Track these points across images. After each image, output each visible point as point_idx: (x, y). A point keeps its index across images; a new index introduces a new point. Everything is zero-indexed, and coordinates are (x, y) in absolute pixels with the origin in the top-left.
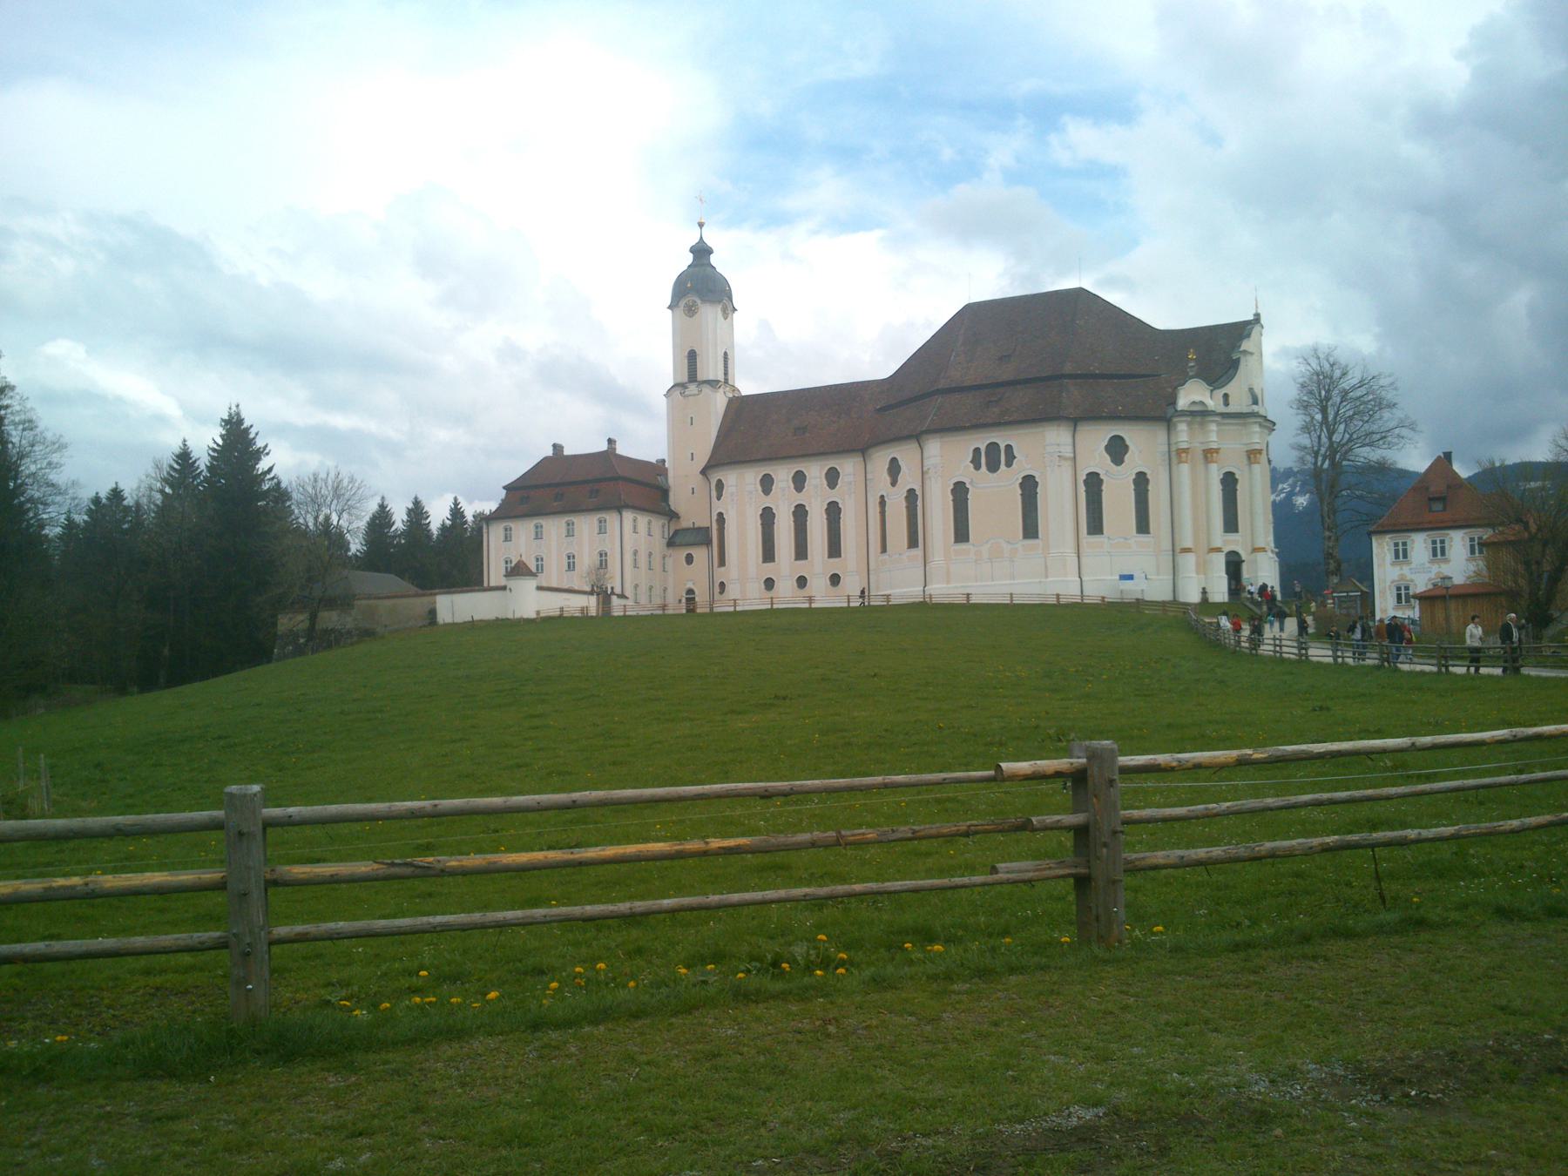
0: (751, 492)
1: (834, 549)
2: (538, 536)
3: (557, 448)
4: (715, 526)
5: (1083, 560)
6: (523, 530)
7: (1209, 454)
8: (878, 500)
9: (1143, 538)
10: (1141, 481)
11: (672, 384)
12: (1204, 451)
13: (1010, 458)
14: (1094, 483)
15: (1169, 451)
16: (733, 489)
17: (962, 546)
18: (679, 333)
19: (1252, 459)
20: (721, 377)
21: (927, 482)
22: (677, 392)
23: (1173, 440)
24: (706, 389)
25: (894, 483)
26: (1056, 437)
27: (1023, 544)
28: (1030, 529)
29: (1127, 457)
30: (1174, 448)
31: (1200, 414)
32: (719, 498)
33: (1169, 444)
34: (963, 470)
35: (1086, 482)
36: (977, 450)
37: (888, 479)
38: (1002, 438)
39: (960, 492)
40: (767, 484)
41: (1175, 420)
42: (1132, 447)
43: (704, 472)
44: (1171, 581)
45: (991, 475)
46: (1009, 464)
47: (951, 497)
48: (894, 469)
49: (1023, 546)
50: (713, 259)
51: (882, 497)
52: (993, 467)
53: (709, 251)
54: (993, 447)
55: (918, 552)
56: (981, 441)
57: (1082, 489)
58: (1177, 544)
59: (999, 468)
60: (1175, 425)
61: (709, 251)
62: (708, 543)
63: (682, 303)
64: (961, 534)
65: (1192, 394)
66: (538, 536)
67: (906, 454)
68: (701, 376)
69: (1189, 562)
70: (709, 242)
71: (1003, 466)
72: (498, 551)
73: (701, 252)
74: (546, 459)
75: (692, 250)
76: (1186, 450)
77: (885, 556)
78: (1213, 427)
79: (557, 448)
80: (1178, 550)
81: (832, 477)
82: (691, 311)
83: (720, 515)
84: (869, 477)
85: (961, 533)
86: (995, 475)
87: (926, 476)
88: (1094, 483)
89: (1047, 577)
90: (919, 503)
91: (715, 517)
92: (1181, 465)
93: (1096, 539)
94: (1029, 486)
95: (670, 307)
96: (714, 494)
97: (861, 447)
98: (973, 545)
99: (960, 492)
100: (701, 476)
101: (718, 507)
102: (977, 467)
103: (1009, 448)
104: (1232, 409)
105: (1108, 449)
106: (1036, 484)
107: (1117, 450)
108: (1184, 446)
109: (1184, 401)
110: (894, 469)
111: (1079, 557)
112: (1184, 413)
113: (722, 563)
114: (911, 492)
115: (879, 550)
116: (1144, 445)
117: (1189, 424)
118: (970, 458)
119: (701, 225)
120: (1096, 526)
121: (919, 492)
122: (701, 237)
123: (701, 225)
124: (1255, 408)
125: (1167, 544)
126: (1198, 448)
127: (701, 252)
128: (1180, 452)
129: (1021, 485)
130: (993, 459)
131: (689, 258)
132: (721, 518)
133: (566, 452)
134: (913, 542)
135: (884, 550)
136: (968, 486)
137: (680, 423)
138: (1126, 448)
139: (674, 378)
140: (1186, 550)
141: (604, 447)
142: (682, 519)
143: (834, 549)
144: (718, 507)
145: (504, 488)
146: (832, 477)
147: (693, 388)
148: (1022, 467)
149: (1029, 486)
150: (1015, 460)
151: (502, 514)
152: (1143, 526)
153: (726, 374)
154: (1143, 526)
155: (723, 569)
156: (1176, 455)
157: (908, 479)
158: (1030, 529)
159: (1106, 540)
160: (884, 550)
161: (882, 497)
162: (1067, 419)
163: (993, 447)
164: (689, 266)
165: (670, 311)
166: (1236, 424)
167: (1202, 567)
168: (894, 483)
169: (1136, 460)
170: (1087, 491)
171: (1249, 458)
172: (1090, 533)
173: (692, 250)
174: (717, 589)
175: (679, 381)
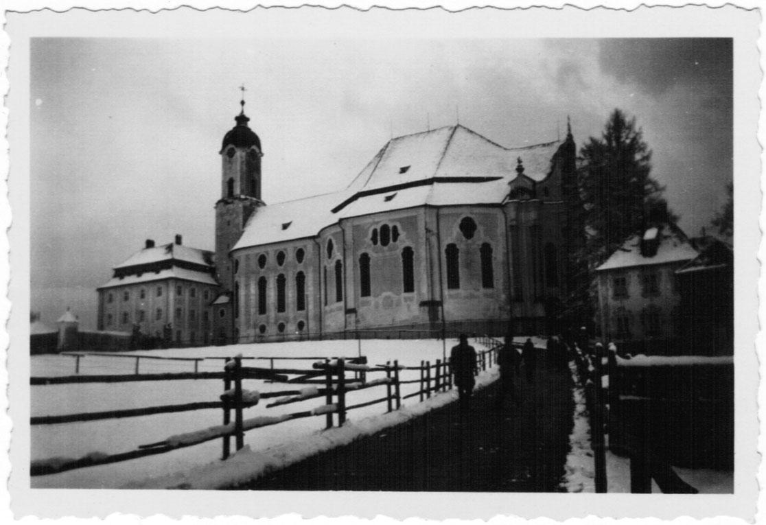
1: (301, 304)
22: (222, 204)
35: (447, 251)
46: (395, 239)
50: (250, 125)
52: (385, 242)
53: (248, 119)
57: (444, 256)
59: (388, 242)
61: (248, 119)
63: (226, 150)
70: (247, 114)
71: (391, 242)
73: (242, 120)
75: (237, 119)
88: (452, 250)
90: (342, 270)
94: (408, 254)
102: (375, 242)
105: (462, 227)
106: (412, 253)
114: (338, 263)
119: (243, 103)
121: (342, 262)
122: (242, 112)
123: (243, 103)
127: (242, 120)
131: (234, 124)
143: (301, 304)
148: (404, 241)
149: (408, 254)
157: (337, 255)
169: (480, 236)
170: (447, 258)
172: (449, 287)
173: (237, 119)
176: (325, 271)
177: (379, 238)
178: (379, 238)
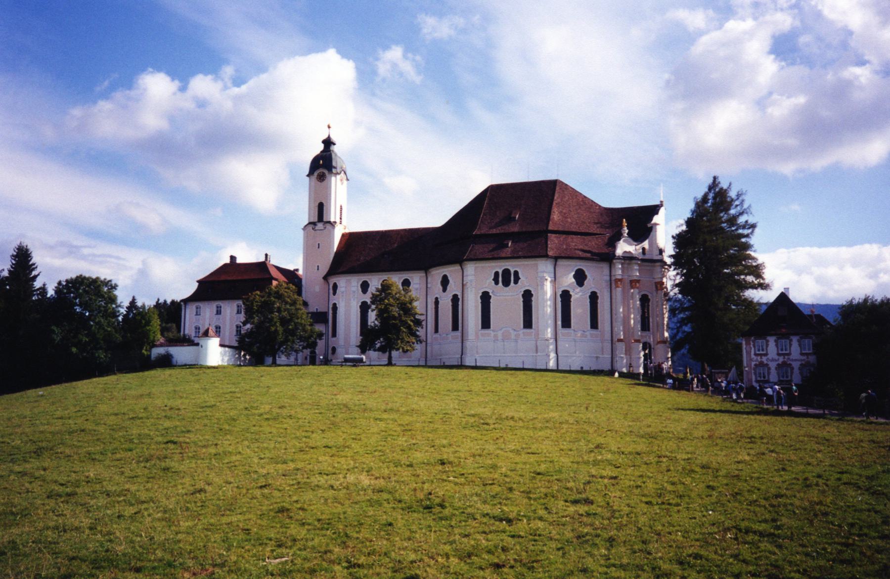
0: (354, 292)
2: (219, 312)
3: (233, 258)
4: (331, 312)
5: (559, 343)
6: (208, 310)
7: (633, 283)
8: (434, 300)
9: (594, 332)
10: (594, 297)
11: (306, 222)
12: (631, 281)
13: (516, 281)
14: (566, 297)
15: (611, 280)
16: (343, 289)
17: (486, 331)
18: (313, 193)
19: (659, 288)
20: (338, 221)
21: (465, 290)
22: (311, 227)
23: (613, 273)
24: (328, 226)
25: (444, 290)
26: (544, 267)
27: (523, 332)
28: (528, 323)
29: (586, 282)
30: (613, 278)
31: (628, 258)
32: (334, 293)
33: (611, 276)
34: (488, 285)
35: (561, 296)
36: (497, 274)
37: (441, 288)
38: (512, 266)
39: (486, 298)
40: (365, 287)
41: (614, 261)
42: (589, 277)
43: (326, 278)
44: (610, 359)
45: (505, 289)
46: (516, 282)
47: (480, 301)
48: (445, 282)
49: (523, 333)
50: (335, 149)
51: (437, 299)
52: (506, 283)
54: (506, 272)
55: (458, 334)
56: (499, 266)
57: (559, 299)
58: (614, 336)
60: (614, 264)
62: (325, 321)
63: (316, 174)
64: (486, 323)
65: (624, 247)
66: (219, 312)
67: (452, 271)
68: (325, 220)
69: (621, 348)
70: (334, 138)
72: (190, 321)
73: (328, 143)
74: (225, 265)
75: (324, 142)
76: (620, 280)
77: (437, 335)
78: (636, 267)
79: (233, 258)
80: (615, 339)
81: (406, 283)
82: (322, 178)
83: (335, 305)
84: (429, 286)
85: (486, 323)
86: (507, 289)
87: (465, 287)
88: (566, 297)
89: (537, 353)
90: (460, 303)
91: (331, 306)
92: (618, 289)
93: (566, 331)
94: (527, 296)
95: (308, 176)
96: (331, 291)
97: (425, 265)
98: (493, 331)
99: (486, 298)
100: (322, 280)
101: (334, 299)
102: (497, 283)
103: (516, 273)
104: (647, 257)
106: (532, 295)
107: (580, 278)
108: (619, 277)
109: (619, 251)
110: (445, 282)
111: (556, 341)
112: (619, 258)
113: (334, 334)
115: (433, 330)
116: (596, 275)
117: (622, 264)
118: (493, 277)
119: (329, 127)
120: (566, 322)
121: (460, 297)
124: (659, 257)
125: (608, 336)
126: (627, 280)
127: (328, 143)
128: (617, 280)
129: (523, 296)
130: (506, 278)
131: (321, 147)
132: (335, 308)
133: (239, 261)
134: (455, 327)
135: (436, 331)
136: (491, 294)
137: (311, 249)
138: (585, 277)
139: (309, 218)
140: (620, 340)
141: (262, 259)
142: (310, 306)
144: (334, 299)
145: (198, 281)
146: (406, 283)
147: (320, 226)
148: (525, 283)
149: (527, 296)
150: (520, 281)
151: (194, 298)
152: (594, 324)
153: (341, 218)
154: (594, 324)
155: (334, 339)
156: (613, 283)
157: (454, 288)
158: (528, 323)
159: (572, 332)
160: (436, 331)
161: (437, 299)
162: (551, 257)
163: (506, 272)
164: (321, 152)
165: (308, 178)
166: (648, 266)
167: (628, 352)
168: (444, 290)
169: (590, 284)
171: (656, 287)
173: (324, 142)
174: (330, 351)
175: (312, 220)
176: (437, 302)
177: (500, 279)
178: (500, 279)
